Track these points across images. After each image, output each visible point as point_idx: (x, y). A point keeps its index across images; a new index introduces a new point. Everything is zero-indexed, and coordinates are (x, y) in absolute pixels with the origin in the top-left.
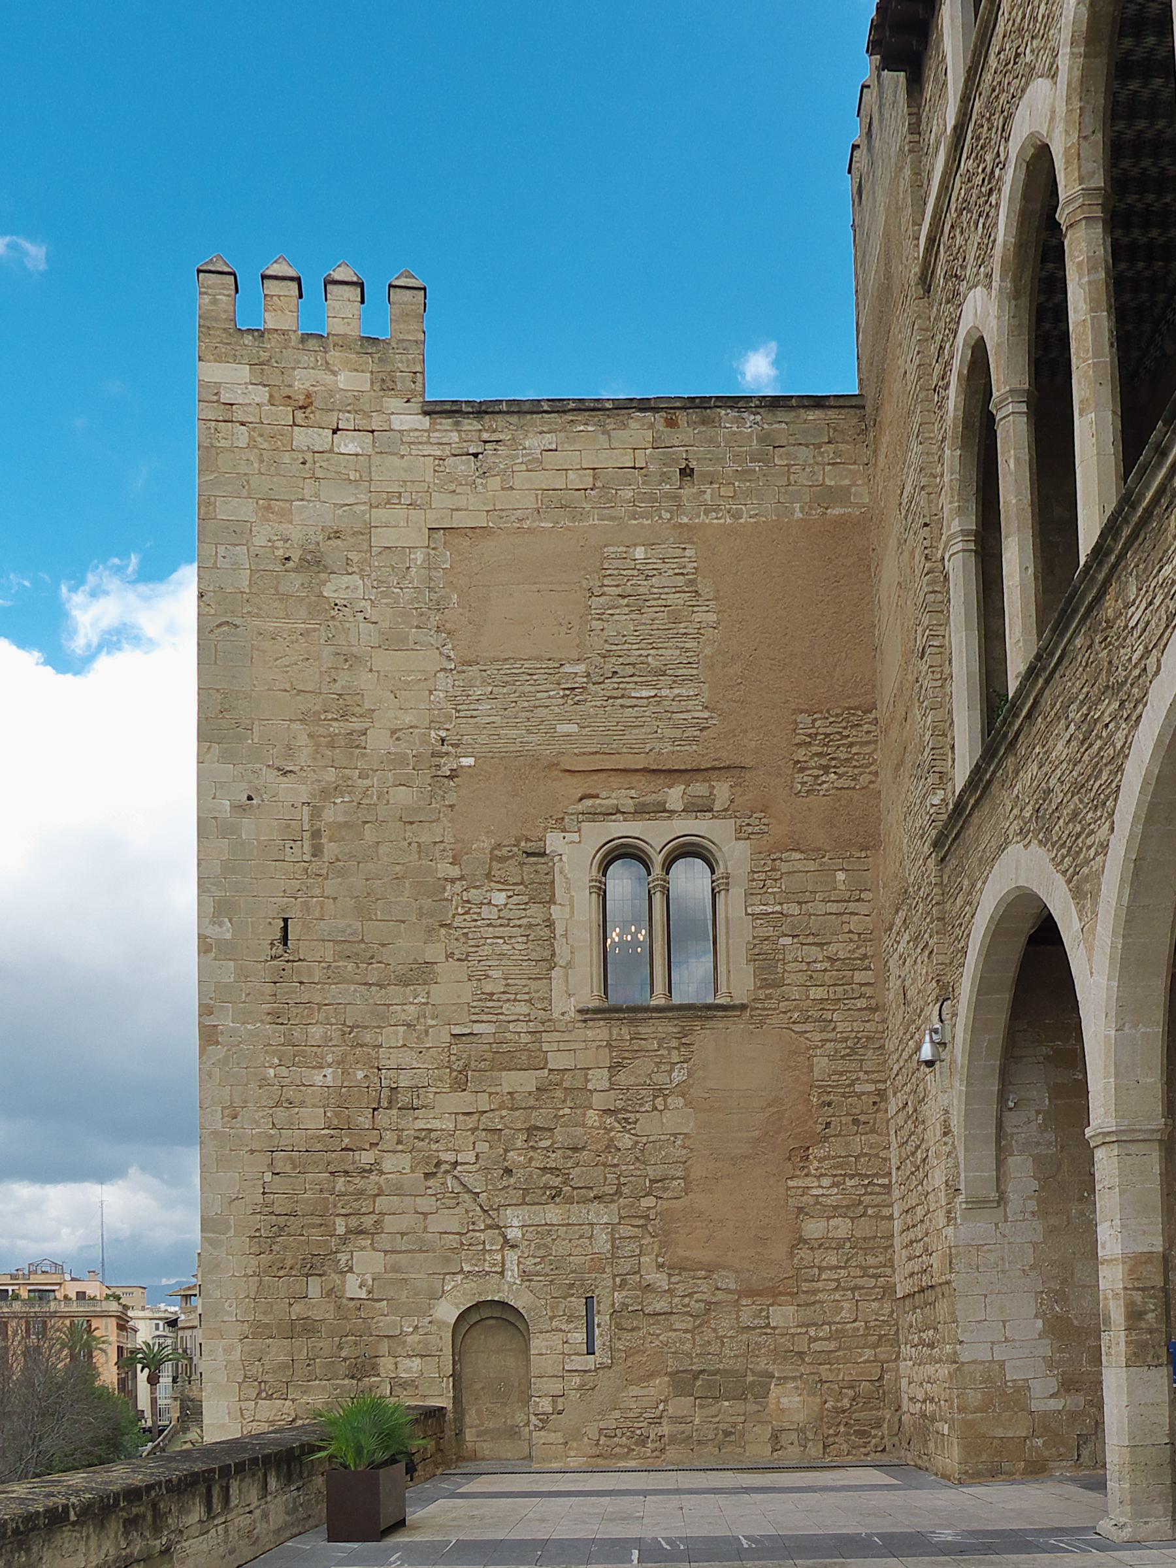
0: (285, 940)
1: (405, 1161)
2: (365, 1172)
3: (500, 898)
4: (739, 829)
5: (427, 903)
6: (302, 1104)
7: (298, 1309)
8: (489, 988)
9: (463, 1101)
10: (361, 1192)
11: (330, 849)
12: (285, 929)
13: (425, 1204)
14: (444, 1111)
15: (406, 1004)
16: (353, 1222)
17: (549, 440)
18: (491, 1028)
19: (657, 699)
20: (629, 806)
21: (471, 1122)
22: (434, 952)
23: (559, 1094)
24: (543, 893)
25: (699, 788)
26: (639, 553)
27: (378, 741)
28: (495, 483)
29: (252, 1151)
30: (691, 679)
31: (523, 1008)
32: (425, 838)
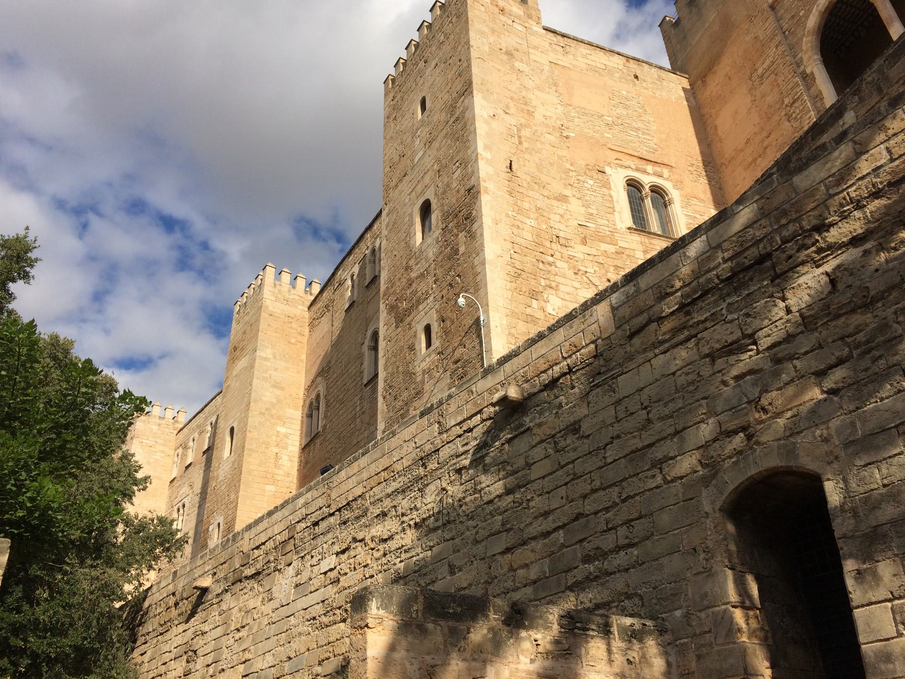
0: (511, 168)
1: (565, 265)
2: (550, 264)
3: (591, 182)
5: (563, 176)
6: (523, 229)
7: (528, 311)
8: (591, 211)
10: (549, 272)
11: (525, 145)
12: (511, 164)
13: (577, 285)
14: (579, 251)
15: (560, 208)
16: (548, 282)
17: (588, 51)
18: (594, 226)
20: (634, 167)
21: (591, 258)
22: (568, 192)
23: (624, 256)
24: (607, 185)
26: (624, 93)
27: (538, 116)
28: (571, 57)
30: (649, 134)
31: (606, 222)
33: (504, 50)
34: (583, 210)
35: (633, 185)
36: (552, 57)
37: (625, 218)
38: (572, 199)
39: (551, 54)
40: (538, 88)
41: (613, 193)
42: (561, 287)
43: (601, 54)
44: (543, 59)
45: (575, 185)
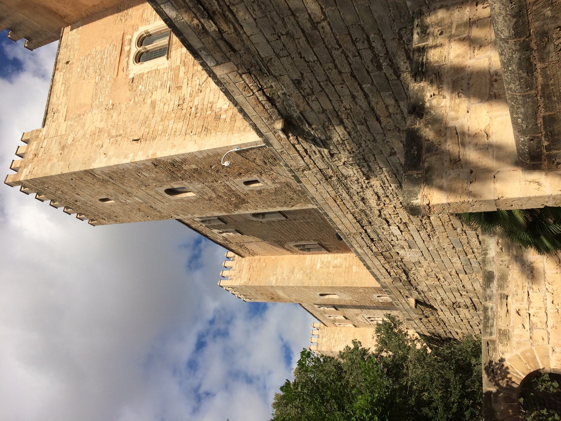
0: (137, 140)
1: (196, 99)
2: (197, 109)
3: (140, 86)
4: (136, 31)
5: (138, 105)
6: (176, 129)
7: (228, 120)
8: (159, 85)
9: (184, 86)
11: (121, 132)
13: (208, 90)
14: (186, 91)
15: (159, 106)
16: (209, 109)
18: (169, 82)
19: (107, 57)
20: (127, 59)
21: (190, 82)
22: (149, 101)
23: (186, 60)
24: (141, 76)
25: (126, 43)
26: (79, 70)
27: (102, 125)
28: (60, 107)
29: (184, 139)
30: (104, 51)
31: (165, 74)
32: (124, 109)
33: (61, 151)
34: (159, 90)
35: (139, 58)
36: (61, 119)
37: (161, 62)
38: (154, 97)
39: (59, 121)
40: (83, 127)
41: (146, 72)
42: (211, 100)
43: (55, 88)
44: (63, 126)
45: (143, 97)
